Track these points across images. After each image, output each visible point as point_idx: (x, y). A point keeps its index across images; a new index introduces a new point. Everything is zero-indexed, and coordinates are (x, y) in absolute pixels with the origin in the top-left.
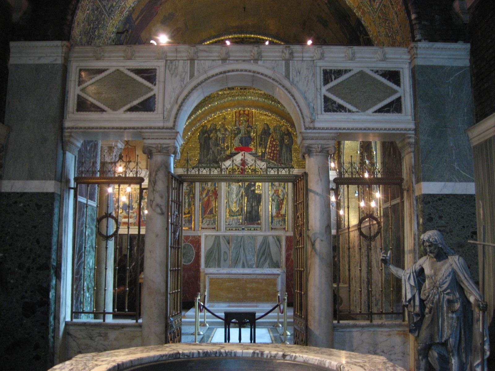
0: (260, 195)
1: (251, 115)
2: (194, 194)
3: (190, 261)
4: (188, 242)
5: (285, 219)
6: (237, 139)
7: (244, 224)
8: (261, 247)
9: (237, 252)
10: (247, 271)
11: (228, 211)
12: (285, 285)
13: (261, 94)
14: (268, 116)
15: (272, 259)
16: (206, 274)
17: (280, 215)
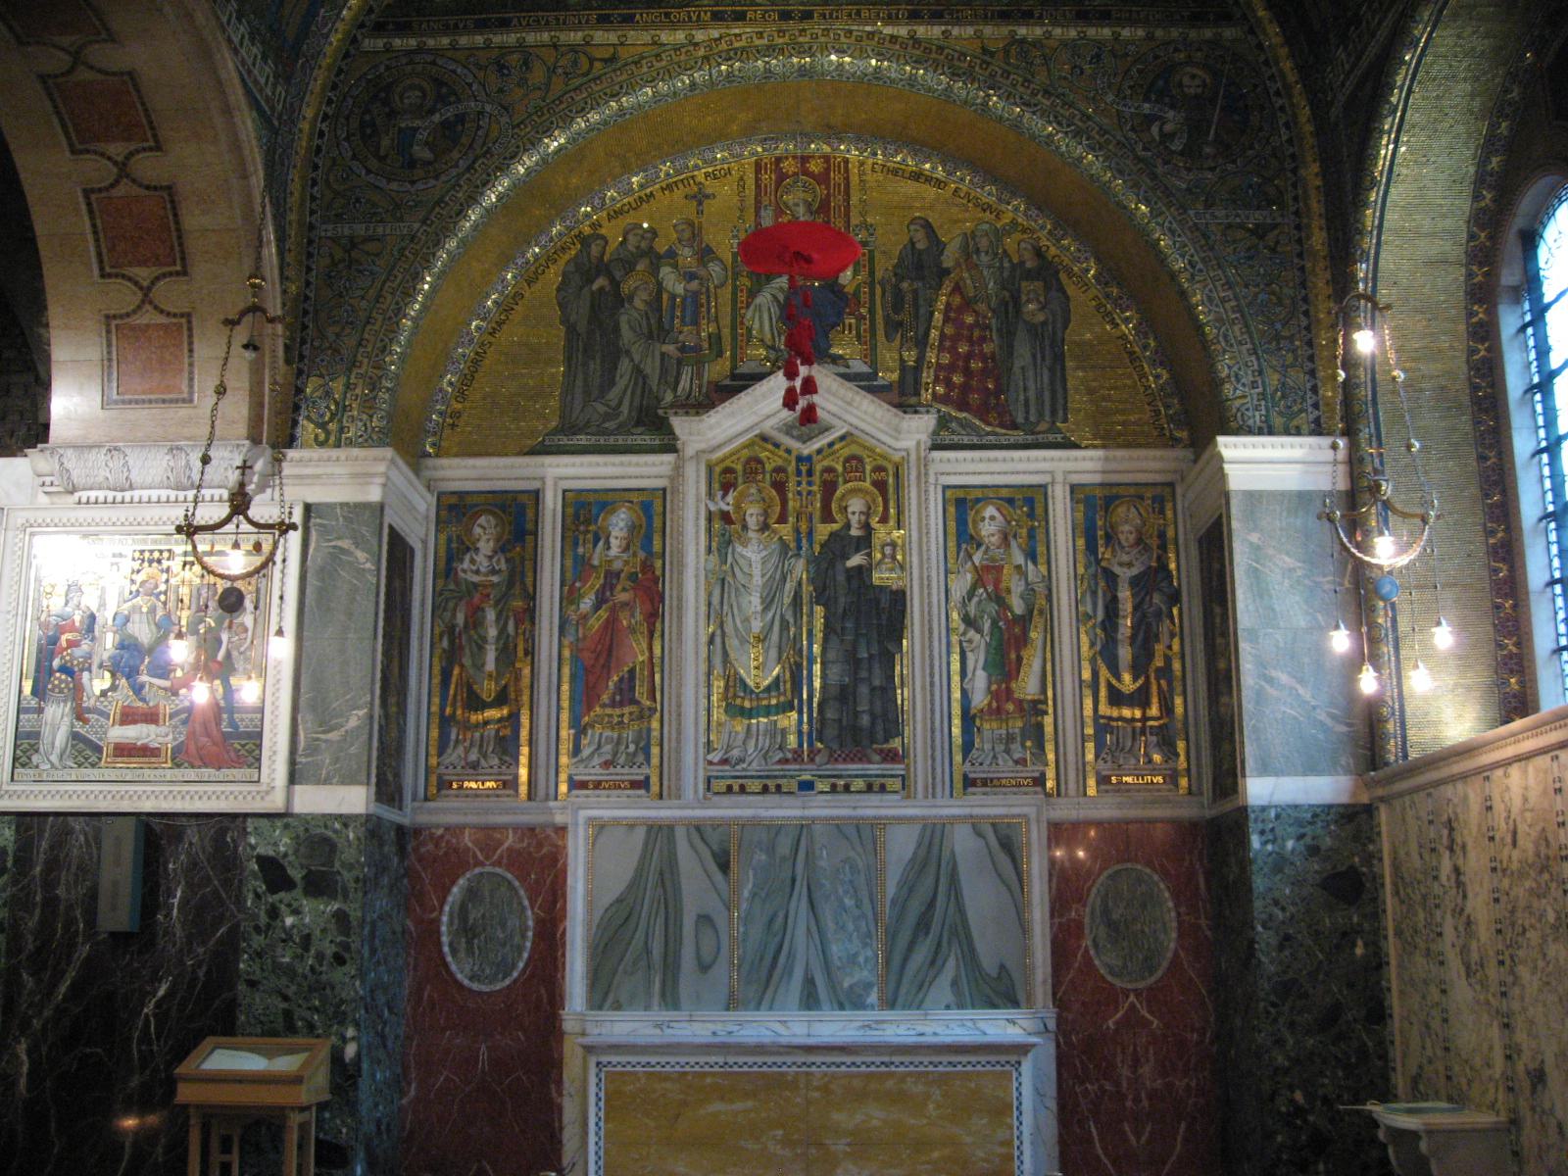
0: (899, 598)
1: (836, 177)
2: (531, 597)
3: (505, 968)
4: (498, 863)
5: (1040, 727)
6: (764, 298)
7: (812, 760)
8: (908, 887)
9: (771, 921)
10: (834, 1027)
11: (718, 685)
12: (1053, 1105)
13: (893, 39)
14: (929, 180)
15: (970, 956)
16: (589, 1049)
17: (1010, 707)
